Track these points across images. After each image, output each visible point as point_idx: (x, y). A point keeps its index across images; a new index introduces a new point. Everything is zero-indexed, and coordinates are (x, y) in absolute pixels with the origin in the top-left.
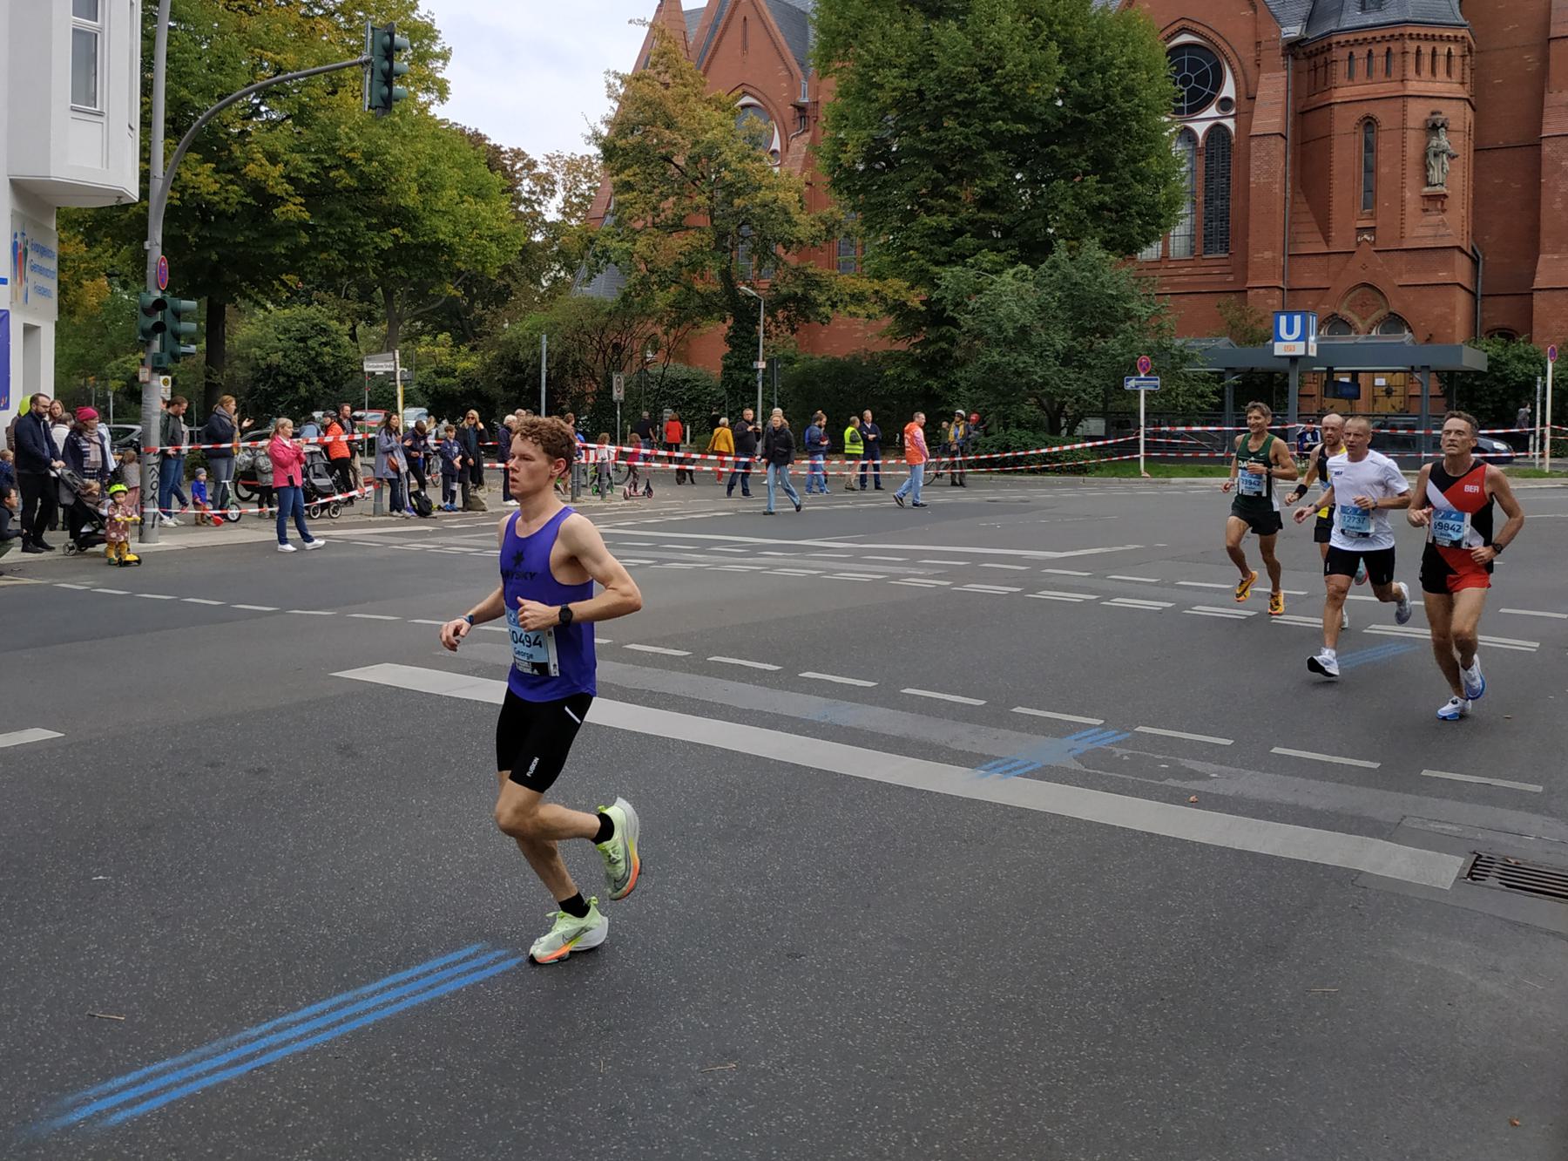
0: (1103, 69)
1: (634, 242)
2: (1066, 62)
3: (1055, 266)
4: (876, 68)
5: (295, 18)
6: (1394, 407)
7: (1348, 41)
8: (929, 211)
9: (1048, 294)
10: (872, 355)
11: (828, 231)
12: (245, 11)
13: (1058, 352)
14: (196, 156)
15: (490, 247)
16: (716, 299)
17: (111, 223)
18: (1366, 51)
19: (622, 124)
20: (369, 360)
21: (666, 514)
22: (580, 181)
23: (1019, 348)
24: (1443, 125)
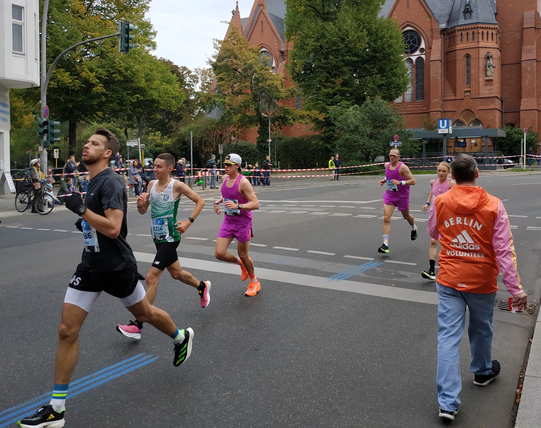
0: (381, 39)
1: (225, 99)
2: (370, 36)
3: (366, 105)
4: (306, 38)
5: (99, 20)
6: (477, 150)
7: (460, 29)
8: (325, 87)
9: (364, 115)
11: (292, 94)
12: (81, 18)
13: (368, 134)
14: (63, 70)
16: (254, 119)
17: (32, 95)
19: (219, 57)
23: (355, 133)
24: (491, 57)
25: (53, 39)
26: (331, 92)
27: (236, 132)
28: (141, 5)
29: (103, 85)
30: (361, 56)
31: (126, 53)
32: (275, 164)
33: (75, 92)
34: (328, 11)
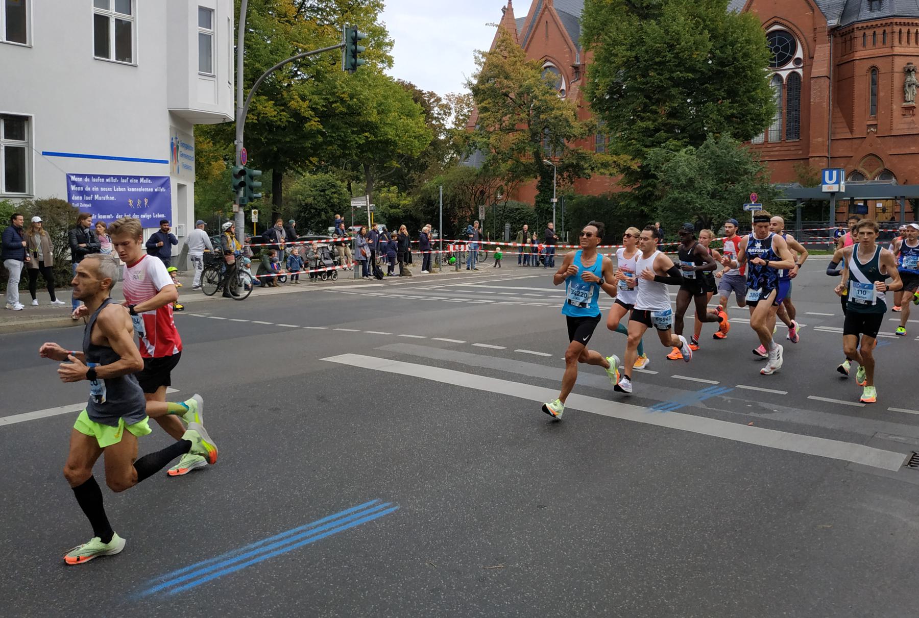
0: (732, 44)
1: (489, 139)
2: (714, 40)
3: (707, 147)
6: (887, 218)
7: (862, 27)
8: (642, 119)
9: (705, 161)
10: (613, 195)
11: (590, 130)
16: (532, 167)
18: (872, 32)
20: (354, 200)
21: (506, 277)
22: (463, 108)
24: (913, 70)
25: (252, 54)
26: (652, 127)
27: (505, 188)
28: (373, 3)
30: (700, 71)
31: (353, 73)
32: (563, 235)
34: (650, 3)
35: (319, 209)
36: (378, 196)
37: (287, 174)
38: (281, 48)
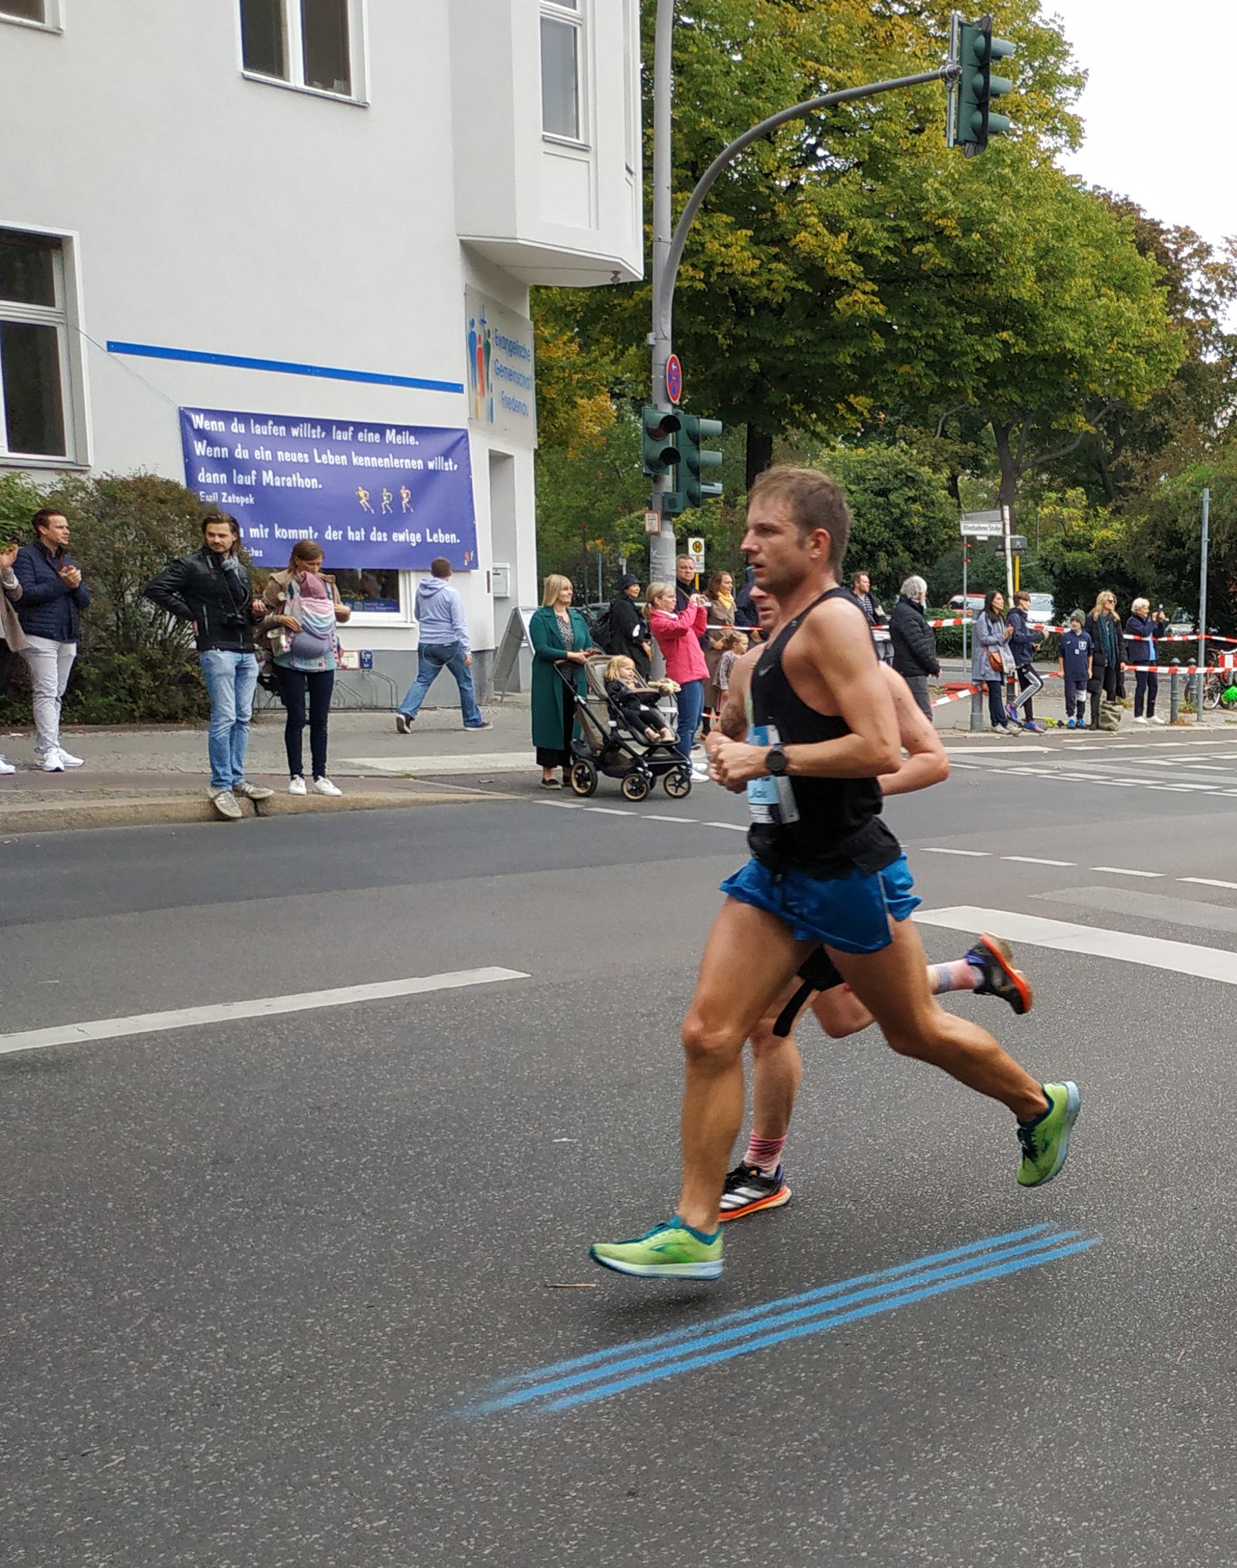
14: (729, 219)
15: (1137, 363)
29: (876, 288)
33: (772, 311)
35: (871, 544)
36: (1031, 517)
37: (785, 440)
38: (771, 76)
